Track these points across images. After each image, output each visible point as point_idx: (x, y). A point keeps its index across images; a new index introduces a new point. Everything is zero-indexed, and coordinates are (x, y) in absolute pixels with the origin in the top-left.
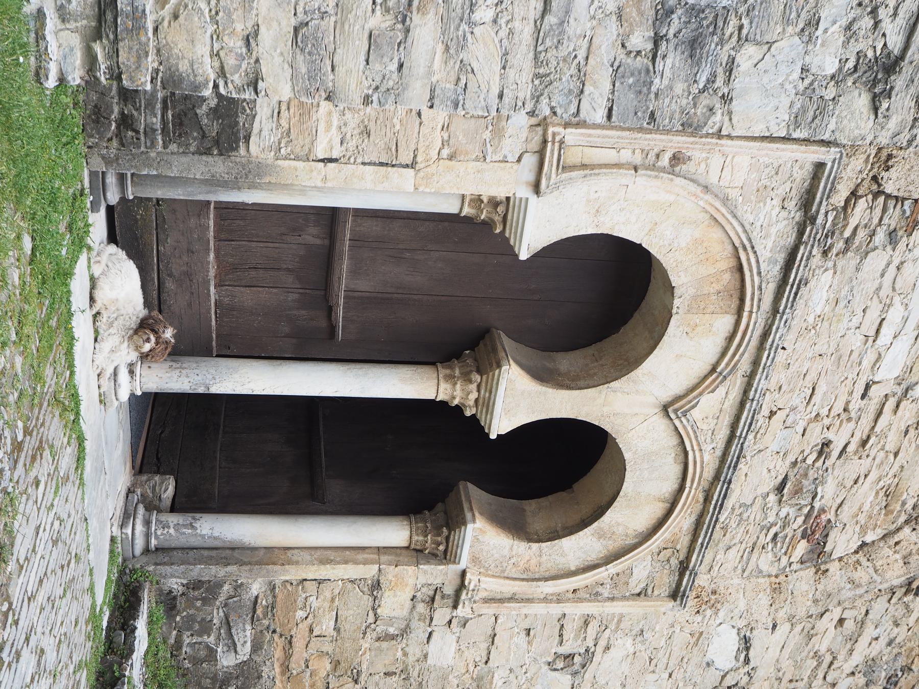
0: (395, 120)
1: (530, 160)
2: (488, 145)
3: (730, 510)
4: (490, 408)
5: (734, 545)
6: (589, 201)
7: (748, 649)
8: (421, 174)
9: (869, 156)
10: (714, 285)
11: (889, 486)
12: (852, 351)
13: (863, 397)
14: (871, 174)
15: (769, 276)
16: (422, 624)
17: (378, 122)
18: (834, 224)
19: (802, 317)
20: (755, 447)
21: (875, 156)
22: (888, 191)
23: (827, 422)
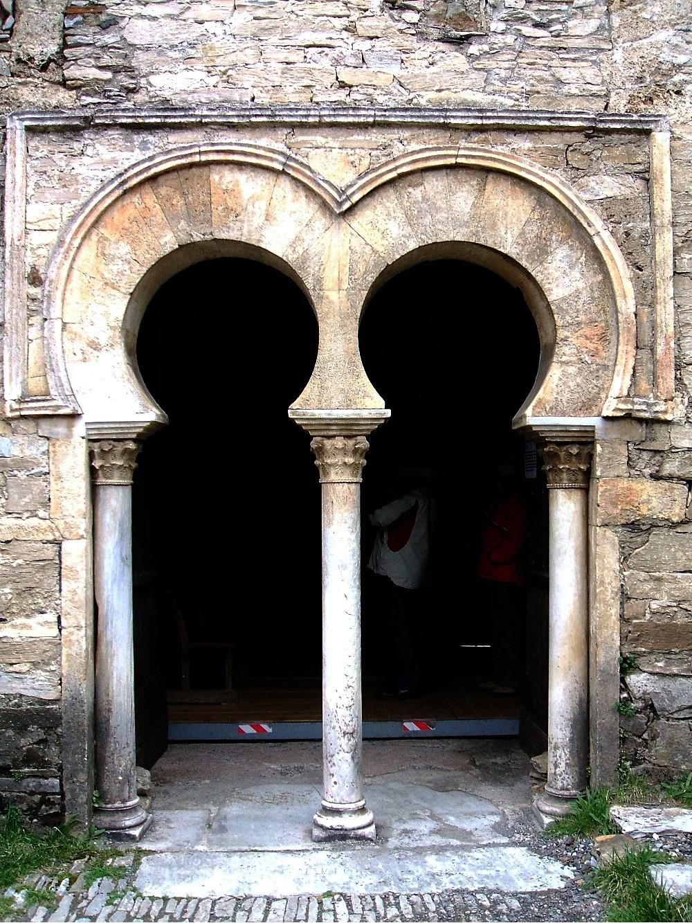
0: (14, 565)
1: (45, 428)
2: (33, 472)
3: (496, 97)
4: (349, 422)
5: (553, 76)
6: (85, 360)
8: (66, 534)
9: (19, 83)
10: (174, 202)
12: (255, 18)
14: (39, 74)
15: (161, 144)
17: (18, 580)
18: (96, 93)
19: (209, 91)
20: (395, 91)
21: (19, 76)
23: (355, 15)
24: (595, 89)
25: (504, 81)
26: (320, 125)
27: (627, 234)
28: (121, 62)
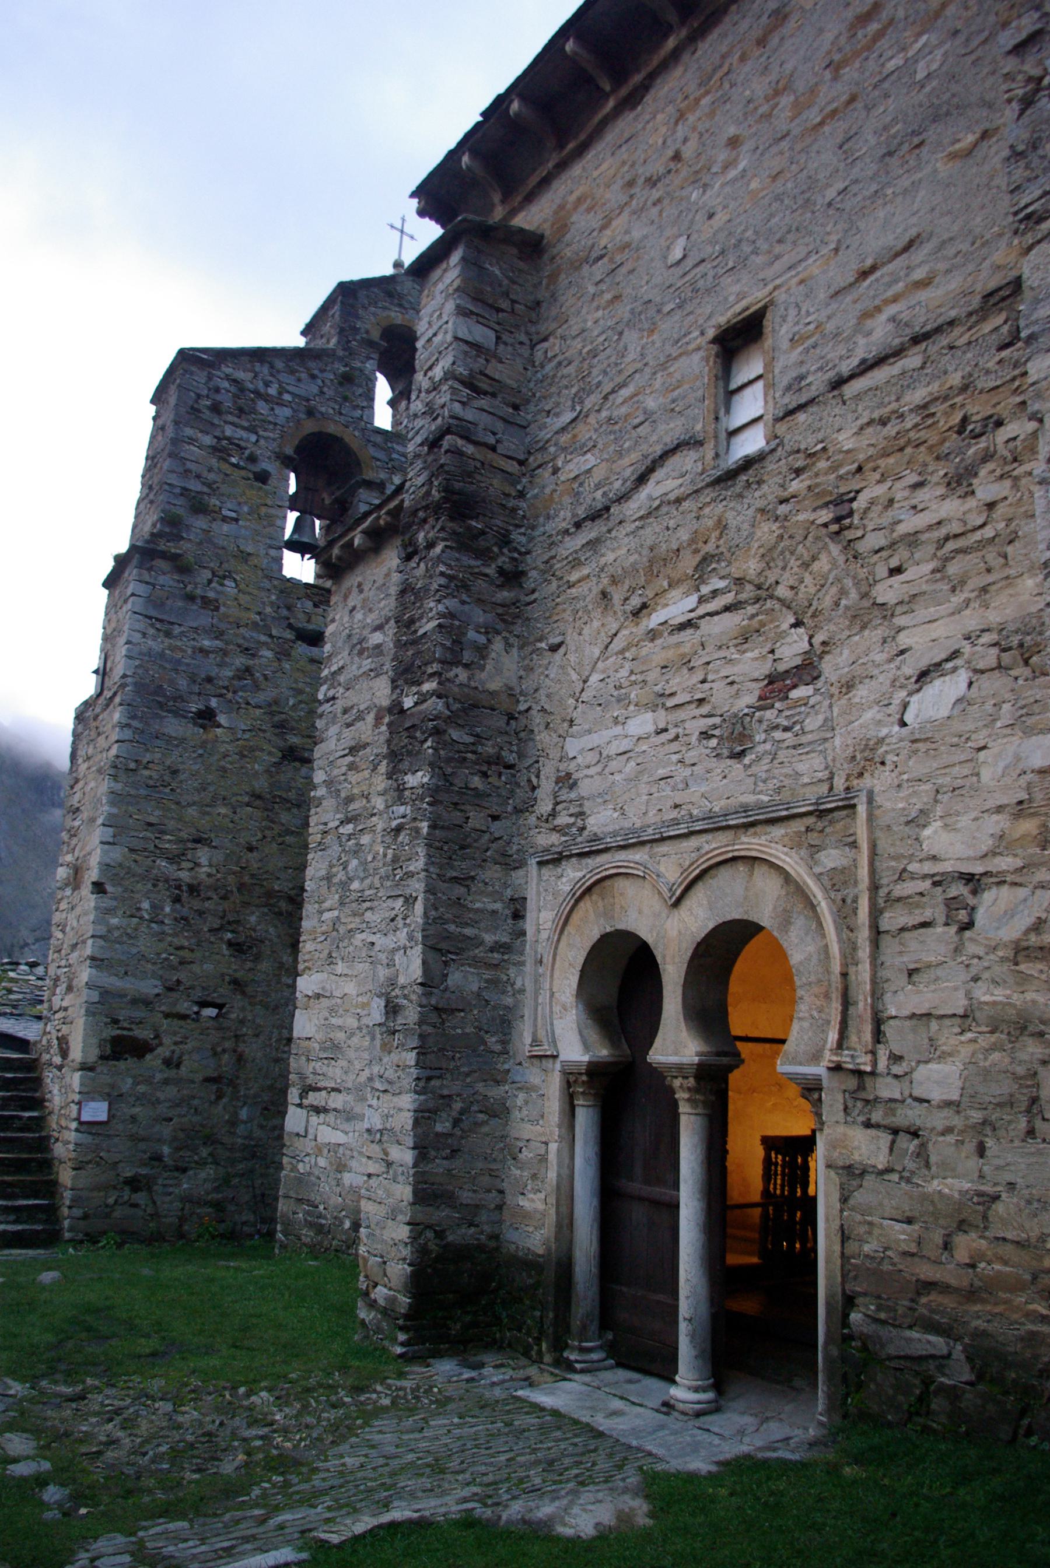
7: (938, 665)
11: (736, 646)
13: (666, 730)
16: (899, 1112)
22: (550, 807)
24: (820, 775)
25: (764, 782)
26: (663, 839)
27: (844, 901)
28: (577, 810)
